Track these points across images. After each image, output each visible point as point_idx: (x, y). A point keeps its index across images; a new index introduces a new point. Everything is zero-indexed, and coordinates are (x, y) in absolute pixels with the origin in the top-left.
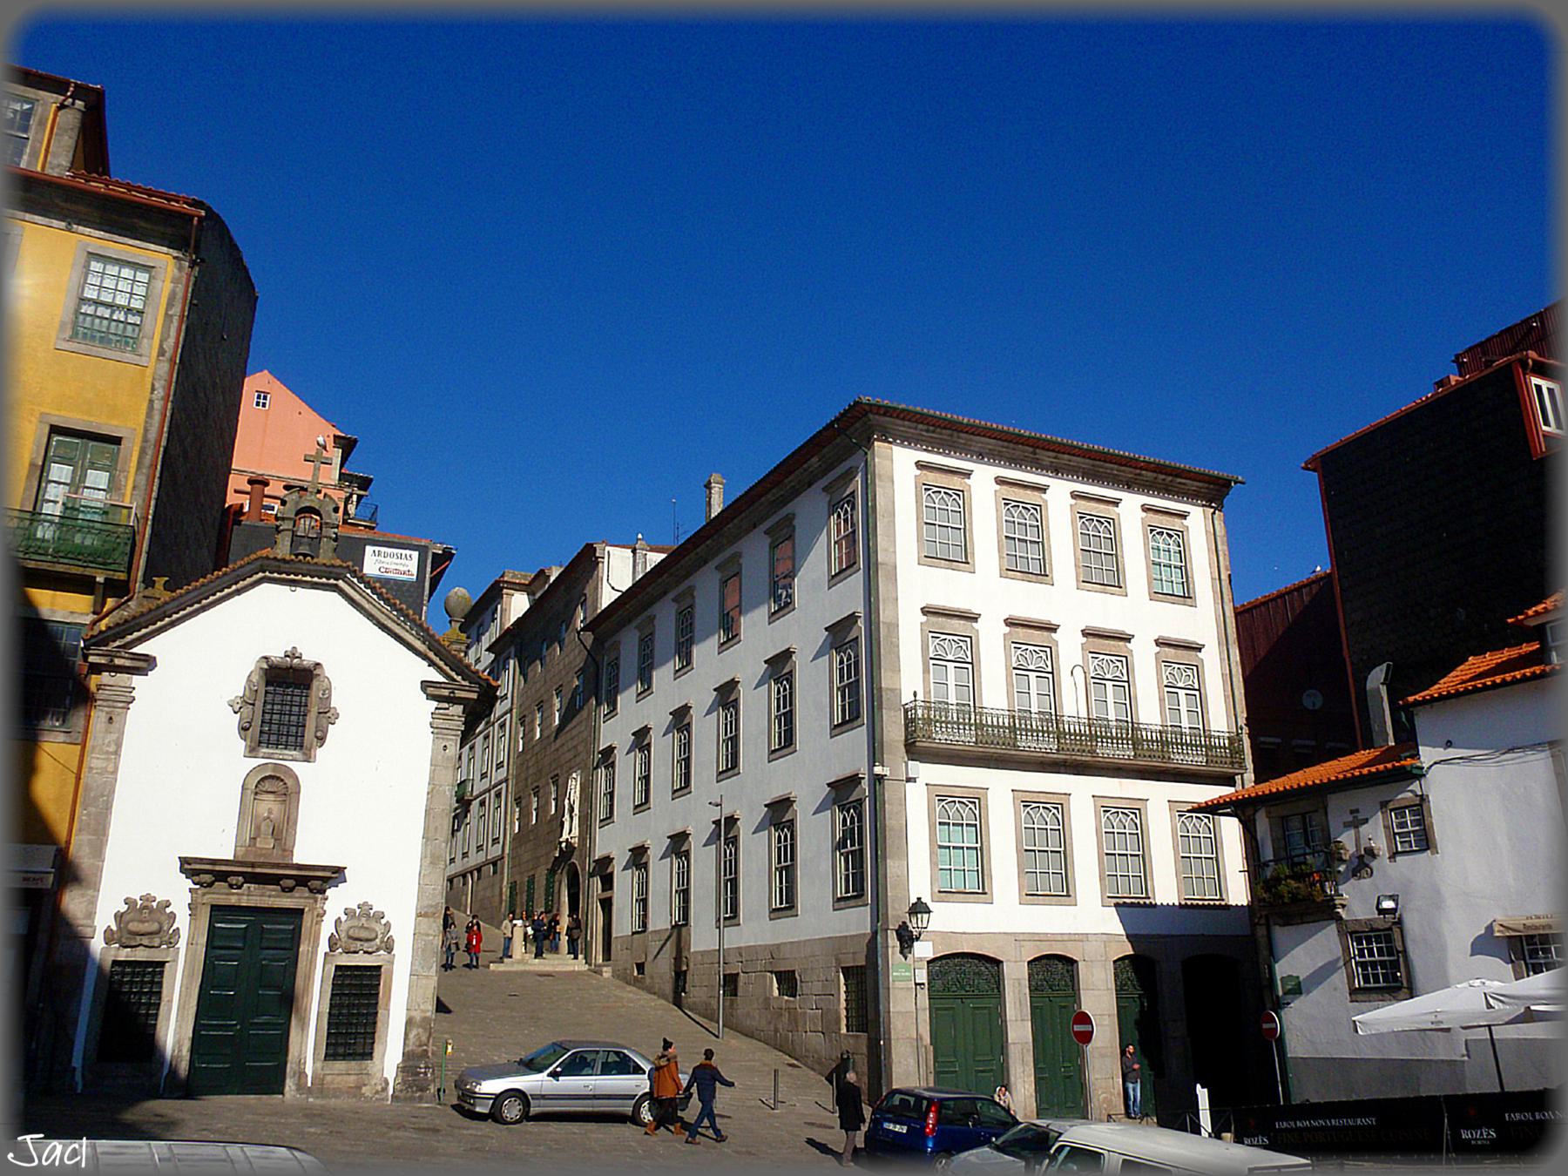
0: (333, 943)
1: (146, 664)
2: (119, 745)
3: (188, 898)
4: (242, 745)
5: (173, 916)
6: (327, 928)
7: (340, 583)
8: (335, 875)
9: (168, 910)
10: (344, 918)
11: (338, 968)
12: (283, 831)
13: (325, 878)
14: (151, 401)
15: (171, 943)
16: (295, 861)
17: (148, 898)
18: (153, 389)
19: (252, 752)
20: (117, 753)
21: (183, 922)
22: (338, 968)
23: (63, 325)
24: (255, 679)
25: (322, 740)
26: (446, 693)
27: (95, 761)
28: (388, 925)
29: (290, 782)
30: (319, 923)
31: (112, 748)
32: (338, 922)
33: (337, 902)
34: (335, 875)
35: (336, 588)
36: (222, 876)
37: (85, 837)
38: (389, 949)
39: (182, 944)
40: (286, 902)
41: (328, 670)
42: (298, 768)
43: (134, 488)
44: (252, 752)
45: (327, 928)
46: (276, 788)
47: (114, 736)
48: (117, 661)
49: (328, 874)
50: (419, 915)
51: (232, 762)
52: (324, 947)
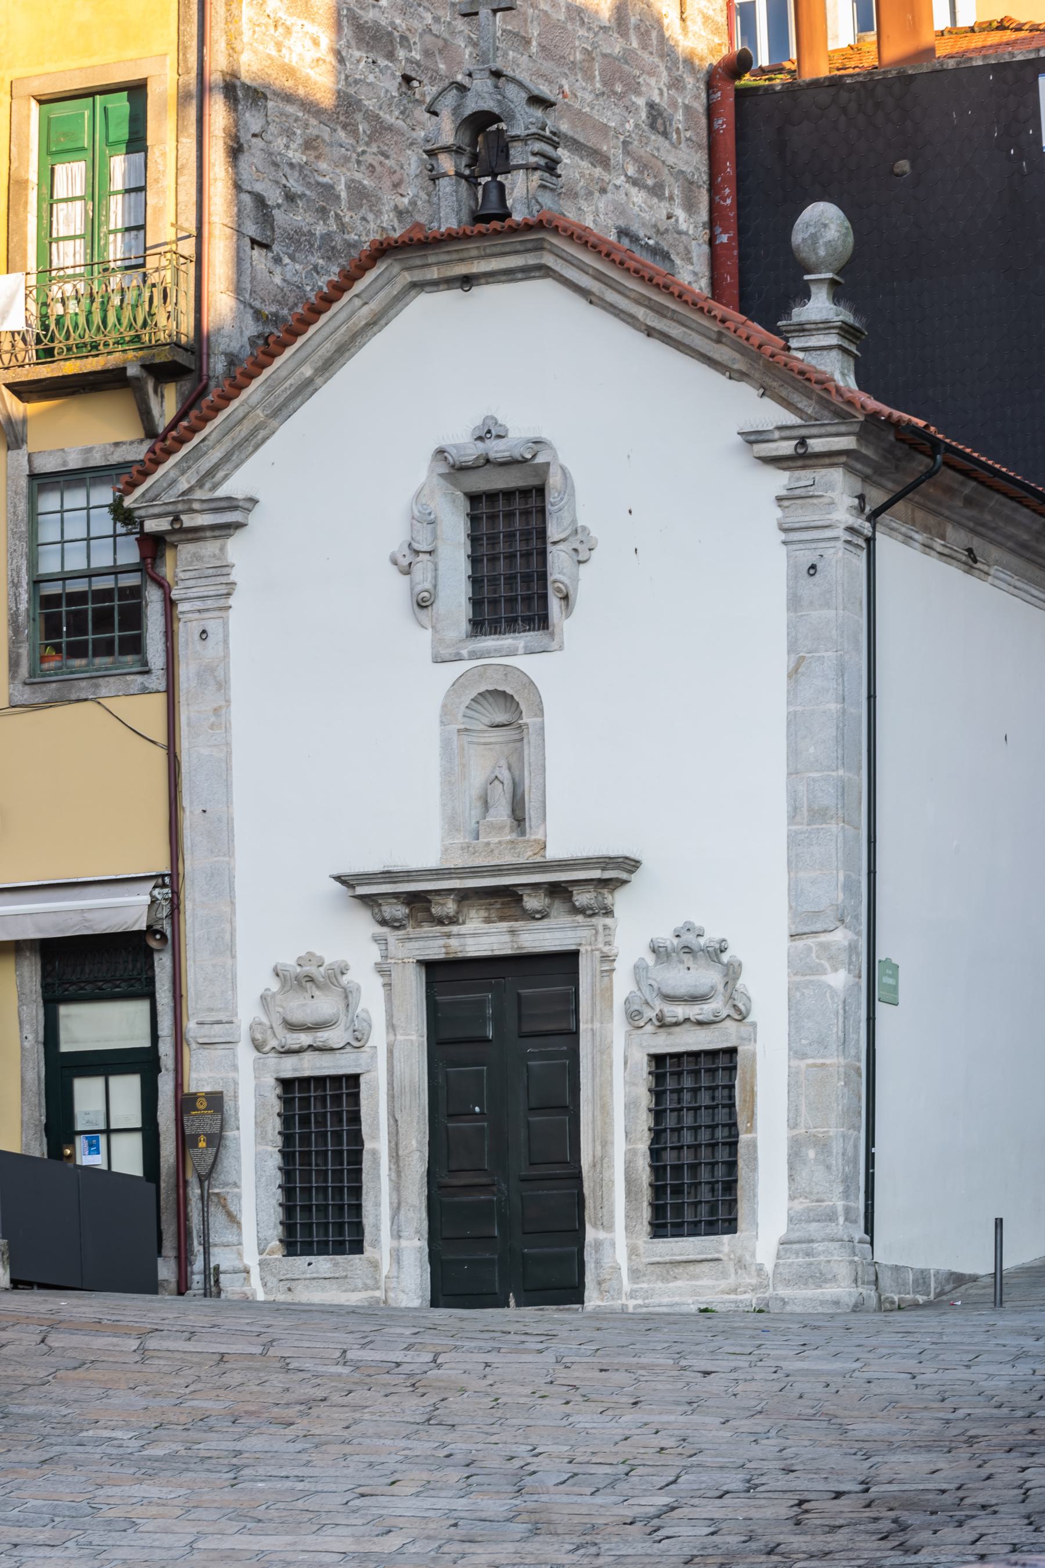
1: (231, 519)
3: (374, 953)
6: (623, 986)
8: (615, 873)
9: (344, 980)
10: (650, 959)
13: (593, 885)
15: (358, 1041)
16: (553, 853)
21: (372, 1000)
26: (787, 448)
32: (639, 970)
34: (615, 873)
35: (544, 271)
36: (419, 903)
38: (741, 1016)
39: (378, 1038)
48: (188, 521)
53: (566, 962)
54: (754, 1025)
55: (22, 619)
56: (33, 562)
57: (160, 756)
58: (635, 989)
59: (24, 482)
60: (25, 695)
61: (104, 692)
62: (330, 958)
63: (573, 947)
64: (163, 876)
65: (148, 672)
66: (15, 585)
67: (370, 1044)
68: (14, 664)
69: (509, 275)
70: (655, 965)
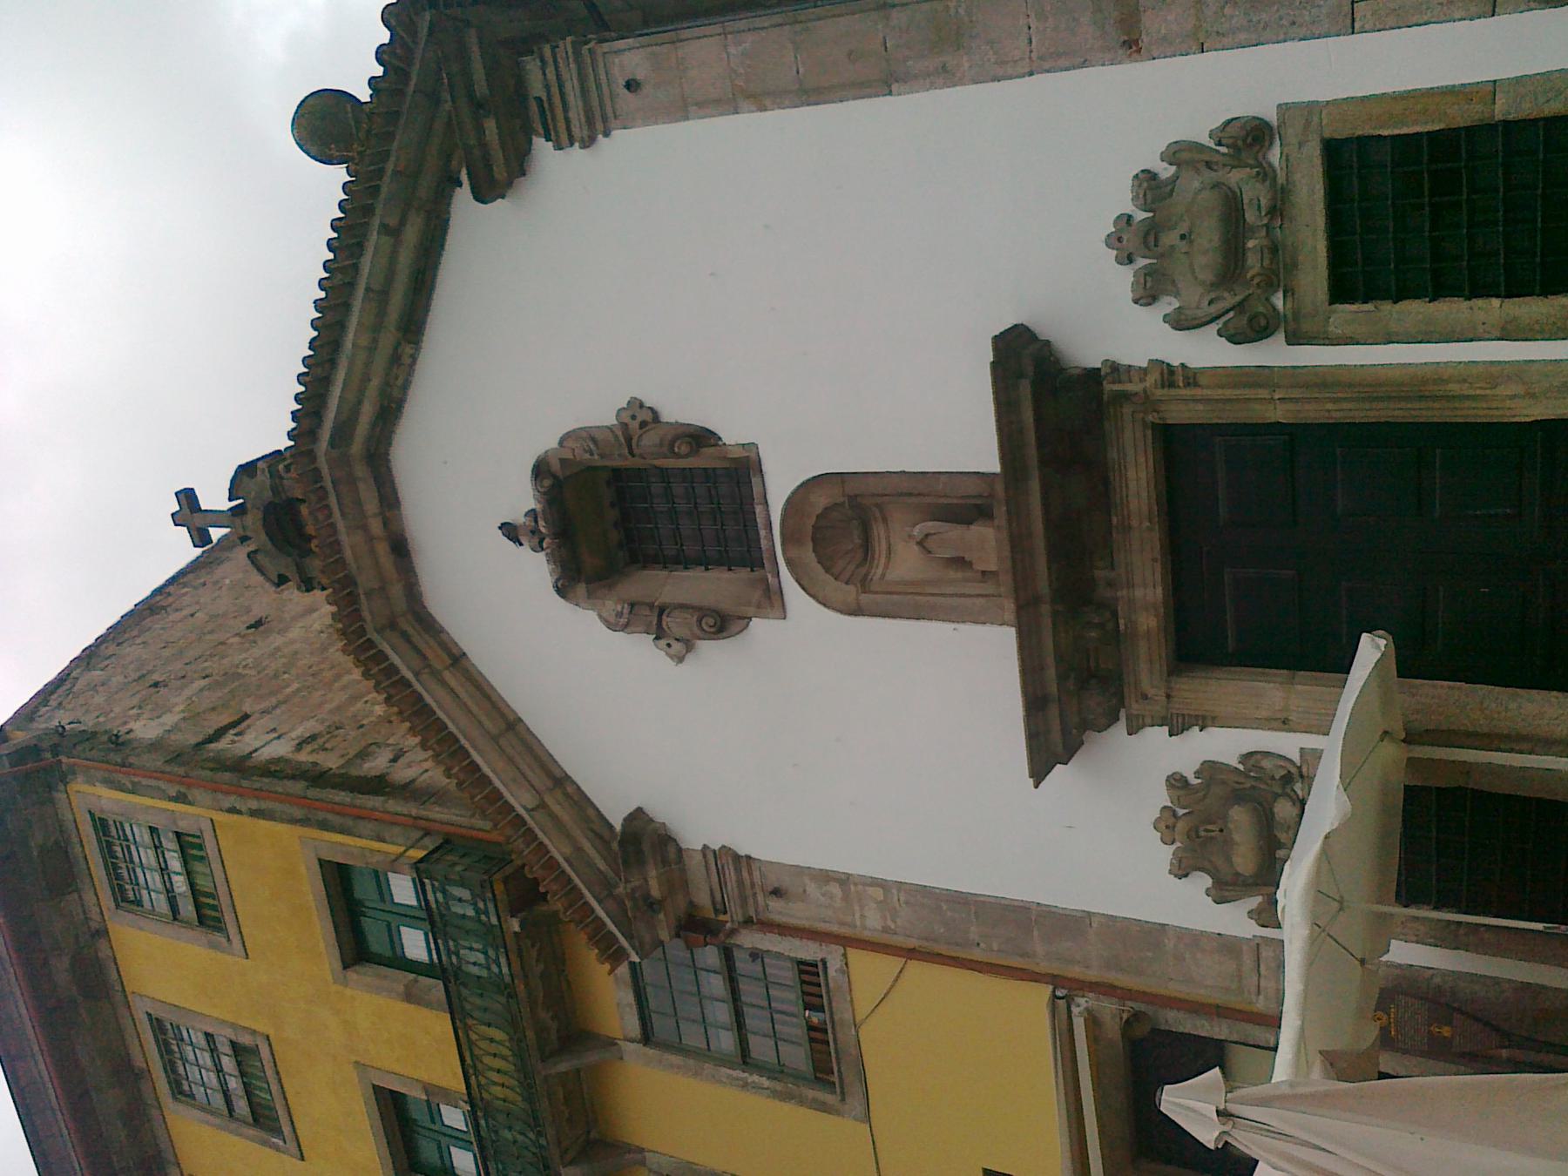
0: (1251, 330)
2: (825, 877)
3: (1156, 735)
4: (760, 627)
5: (1210, 770)
6: (1207, 351)
7: (357, 447)
10: (1168, 304)
11: (1342, 290)
12: (947, 502)
14: (255, 813)
17: (1167, 825)
18: (232, 810)
19: (772, 601)
20: (844, 880)
21: (1224, 745)
22: (1342, 290)
23: (213, 946)
24: (611, 606)
25: (701, 438)
27: (871, 921)
28: (1180, 154)
29: (820, 501)
30: (1191, 377)
31: (835, 889)
32: (1181, 322)
33: (1118, 330)
35: (378, 458)
37: (1040, 949)
40: (1137, 479)
41: (546, 441)
42: (779, 486)
43: (381, 839)
44: (772, 601)
45: (1207, 351)
46: (852, 532)
47: (812, 888)
49: (1025, 389)
50: (1132, 46)
51: (805, 641)
52: (1274, 353)
53: (1174, 443)
54: (1283, 109)
55: (778, 1086)
56: (723, 1061)
57: (916, 968)
58: (1214, 327)
59: (650, 1052)
60: (854, 1103)
61: (848, 1016)
62: (1163, 798)
63: (1149, 432)
64: (1055, 997)
65: (824, 962)
66: (745, 1085)
67: (1296, 758)
68: (824, 1108)
69: (389, 499)
70: (1177, 295)
